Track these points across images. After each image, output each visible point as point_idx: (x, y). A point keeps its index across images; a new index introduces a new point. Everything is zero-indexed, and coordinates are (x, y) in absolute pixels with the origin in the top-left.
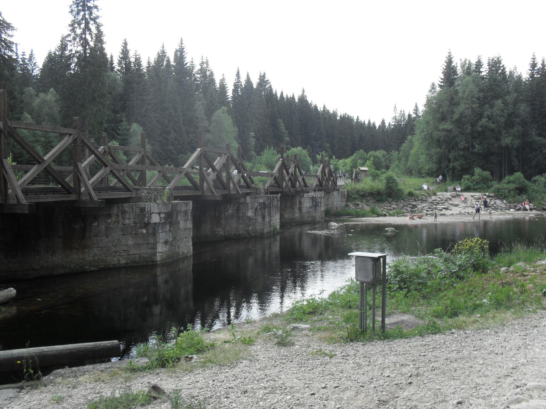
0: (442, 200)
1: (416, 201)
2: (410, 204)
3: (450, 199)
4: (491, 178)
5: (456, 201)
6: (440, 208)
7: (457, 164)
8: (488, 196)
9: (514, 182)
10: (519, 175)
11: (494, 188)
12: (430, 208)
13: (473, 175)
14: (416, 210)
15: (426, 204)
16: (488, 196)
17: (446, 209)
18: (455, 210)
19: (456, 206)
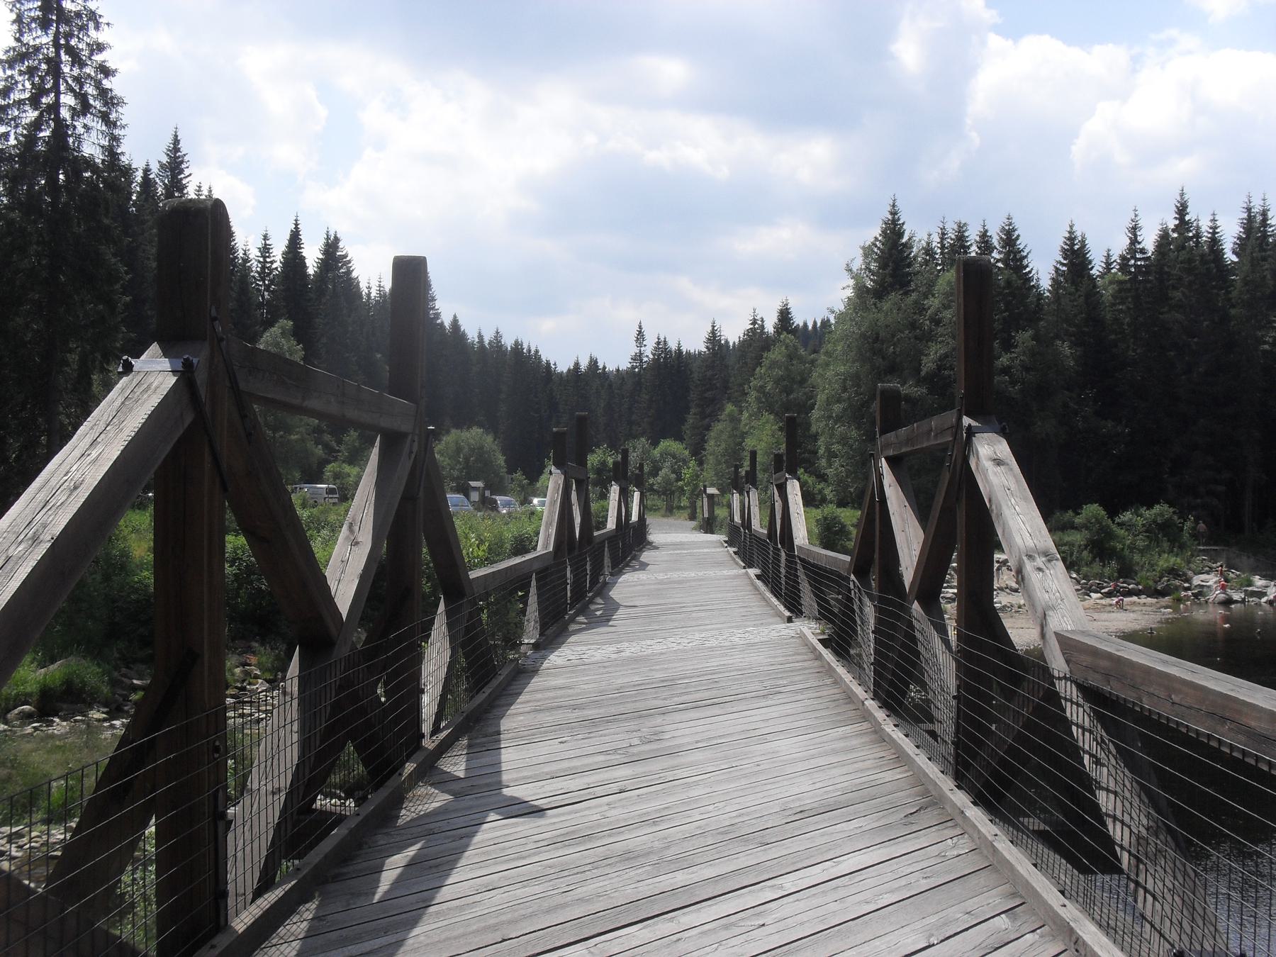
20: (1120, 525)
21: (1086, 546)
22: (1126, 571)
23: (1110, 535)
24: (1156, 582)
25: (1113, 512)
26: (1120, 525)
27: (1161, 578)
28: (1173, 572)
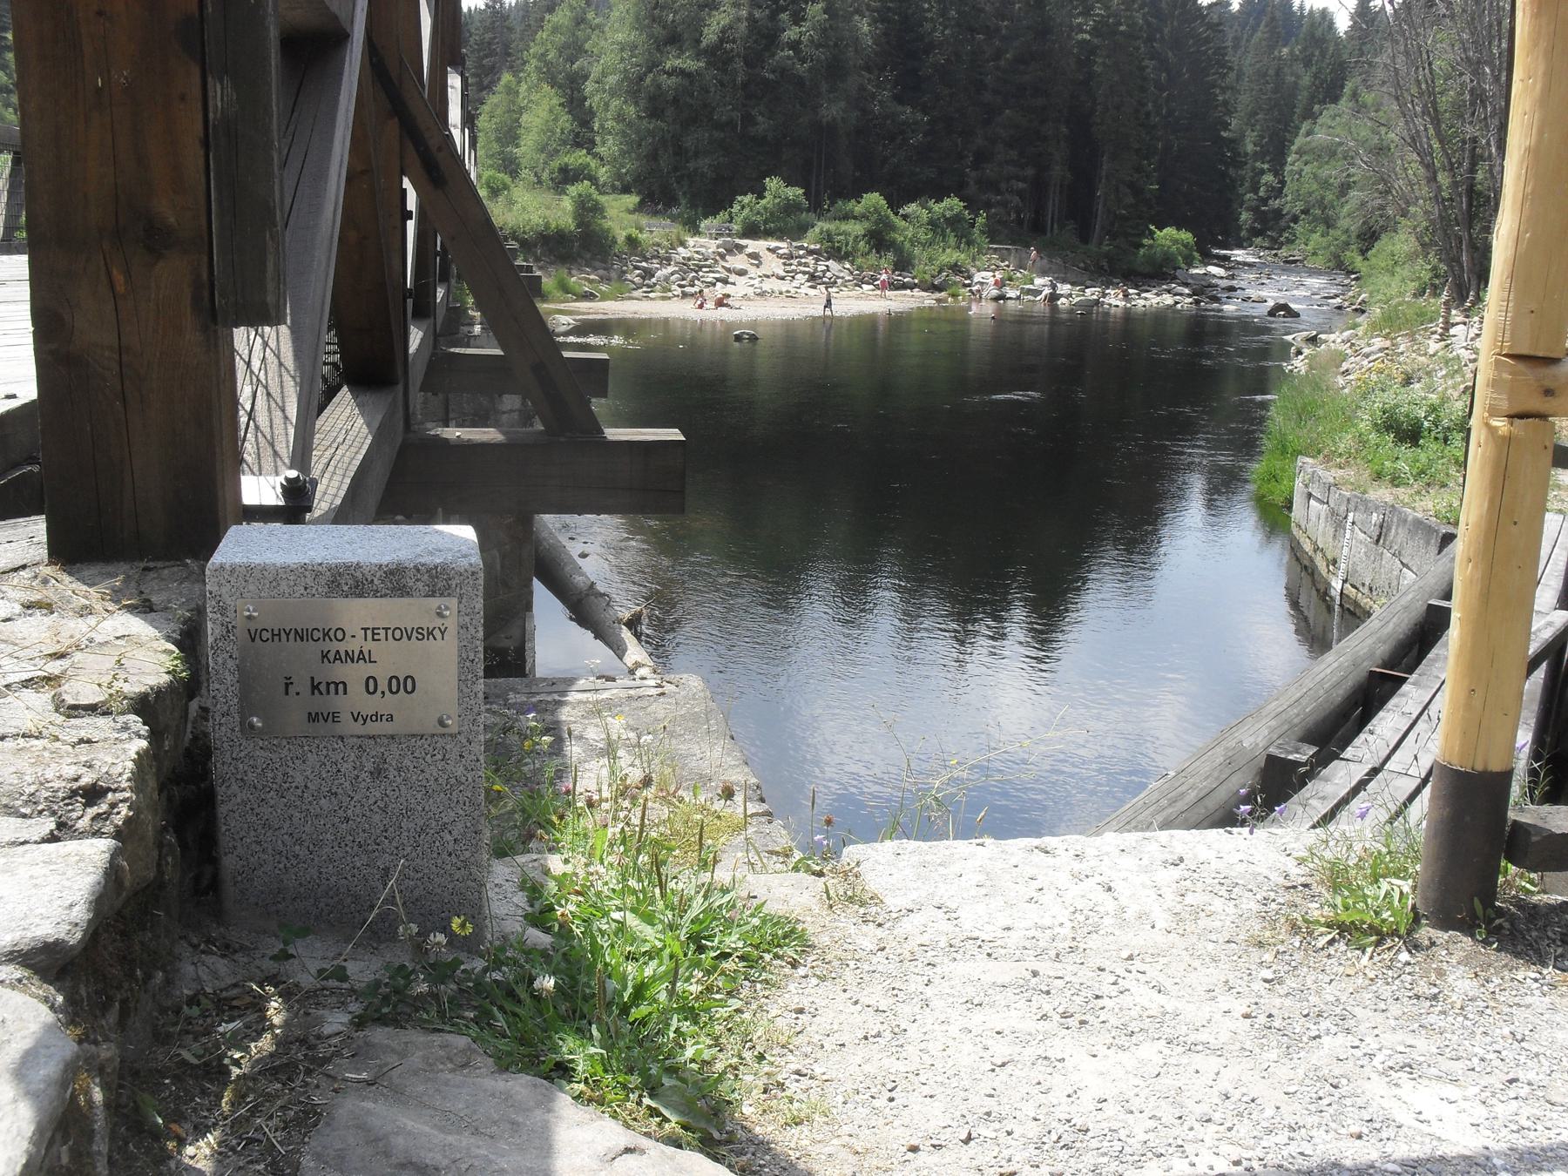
0: (706, 260)
1: (646, 260)
2: (636, 268)
3: (723, 257)
4: (806, 204)
5: (737, 261)
6: (709, 280)
7: (704, 164)
8: (811, 252)
9: (863, 217)
10: (874, 199)
11: (817, 230)
12: (683, 279)
13: (761, 196)
14: (655, 284)
15: (670, 269)
16: (811, 252)
17: (725, 281)
18: (740, 287)
19: (742, 273)
20: (905, 217)
21: (864, 236)
22: (903, 264)
23: (891, 227)
24: (933, 277)
25: (895, 205)
26: (905, 217)
27: (940, 272)
28: (956, 268)
